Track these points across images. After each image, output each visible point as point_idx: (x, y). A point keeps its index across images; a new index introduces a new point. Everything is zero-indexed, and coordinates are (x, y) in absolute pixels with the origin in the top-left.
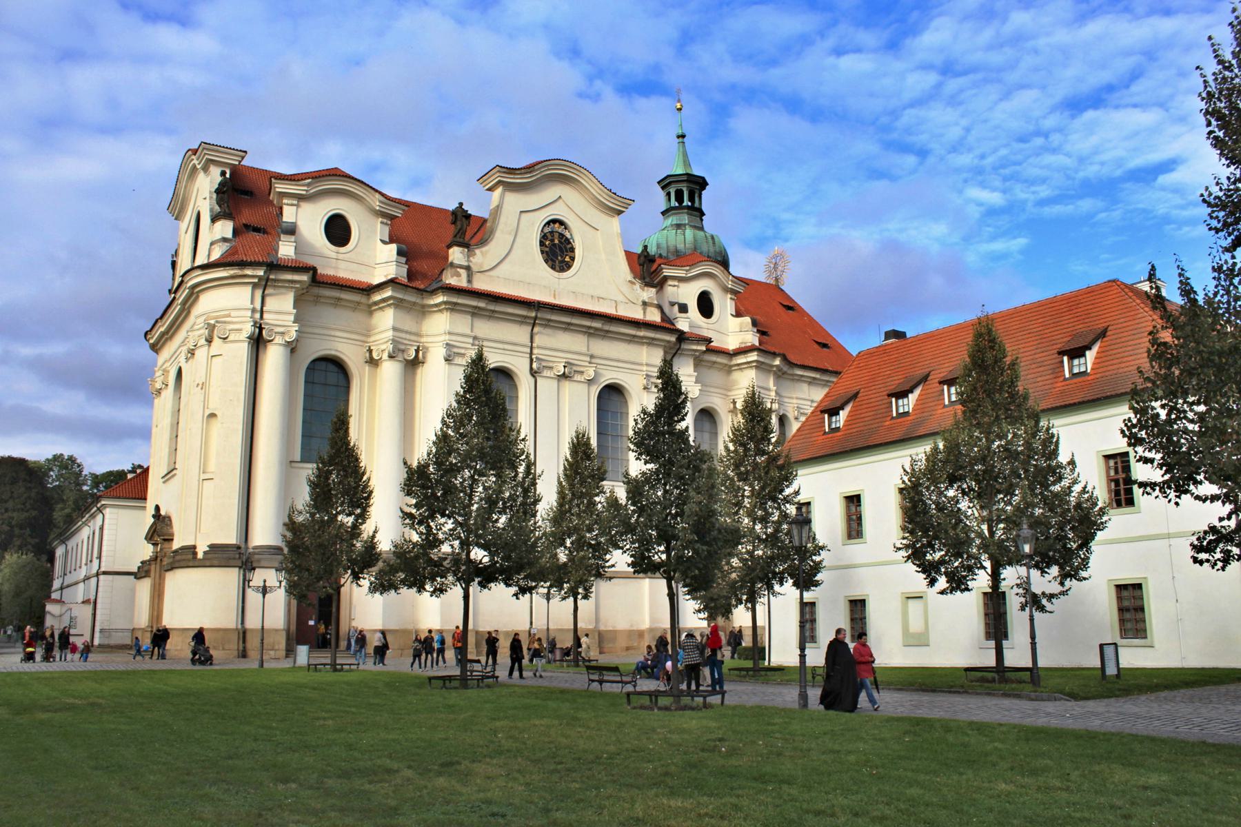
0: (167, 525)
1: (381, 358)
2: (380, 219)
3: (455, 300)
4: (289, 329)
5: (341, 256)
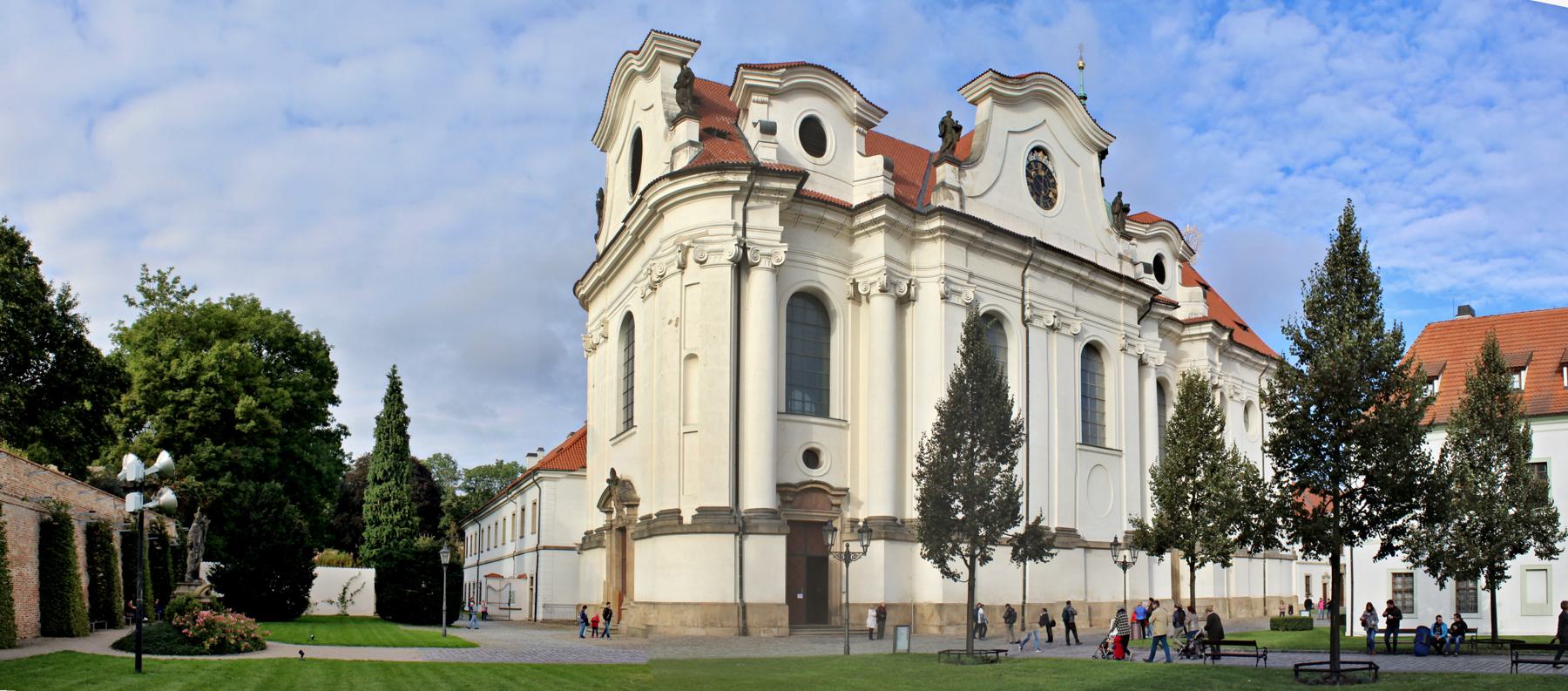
1: (869, 293)
2: (857, 127)
3: (953, 226)
5: (818, 169)
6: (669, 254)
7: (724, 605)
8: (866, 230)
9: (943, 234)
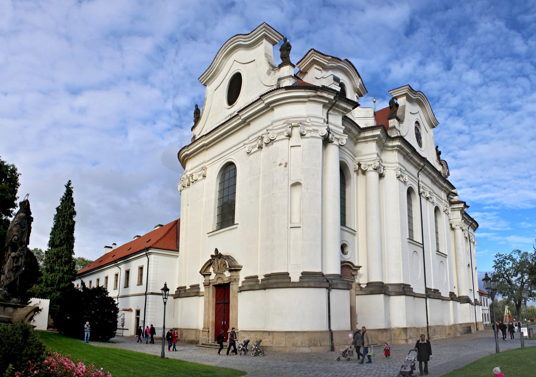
0: (232, 260)
1: (367, 170)
2: (357, 95)
4: (342, 137)
6: (280, 128)
7: (321, 332)
8: (367, 140)
9: (398, 149)
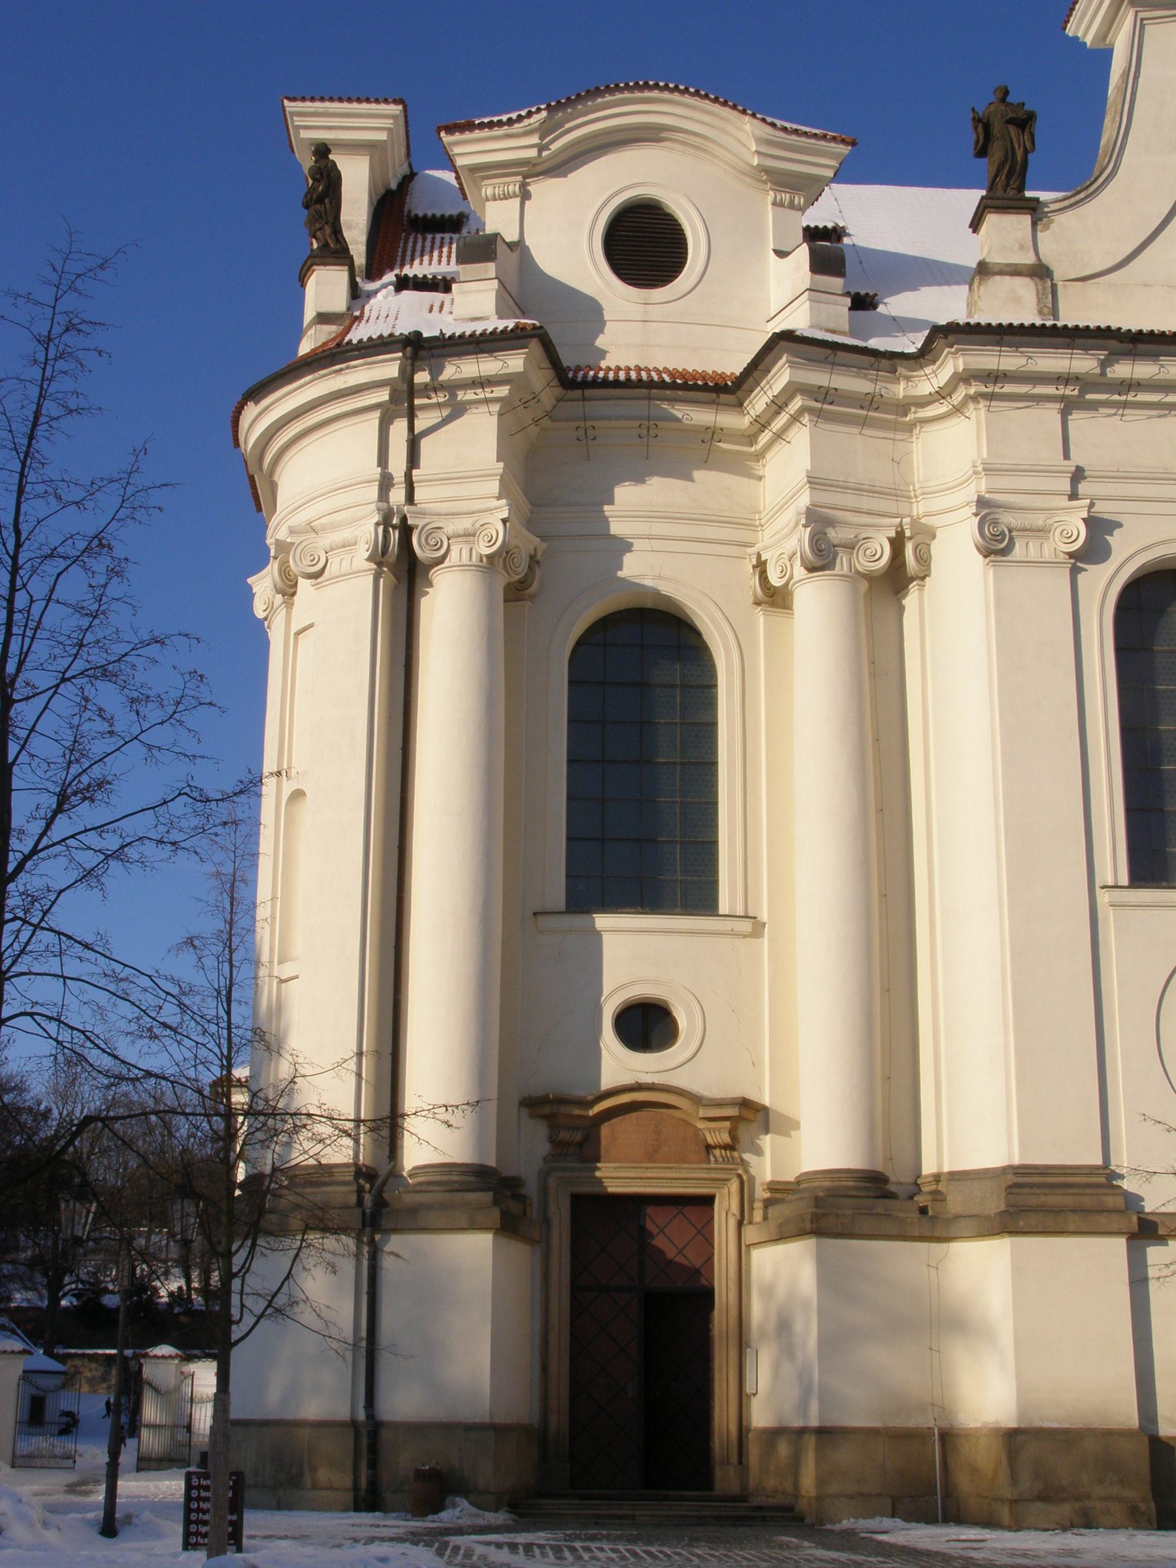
9: (972, 391)
